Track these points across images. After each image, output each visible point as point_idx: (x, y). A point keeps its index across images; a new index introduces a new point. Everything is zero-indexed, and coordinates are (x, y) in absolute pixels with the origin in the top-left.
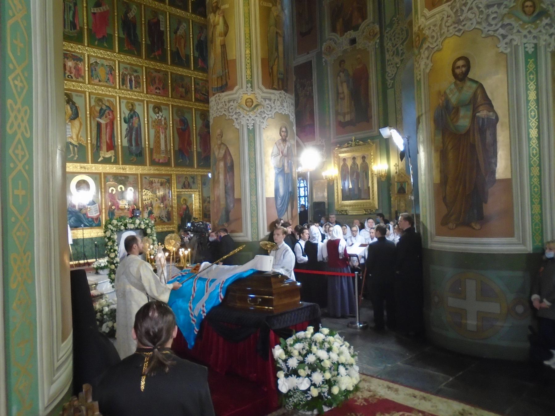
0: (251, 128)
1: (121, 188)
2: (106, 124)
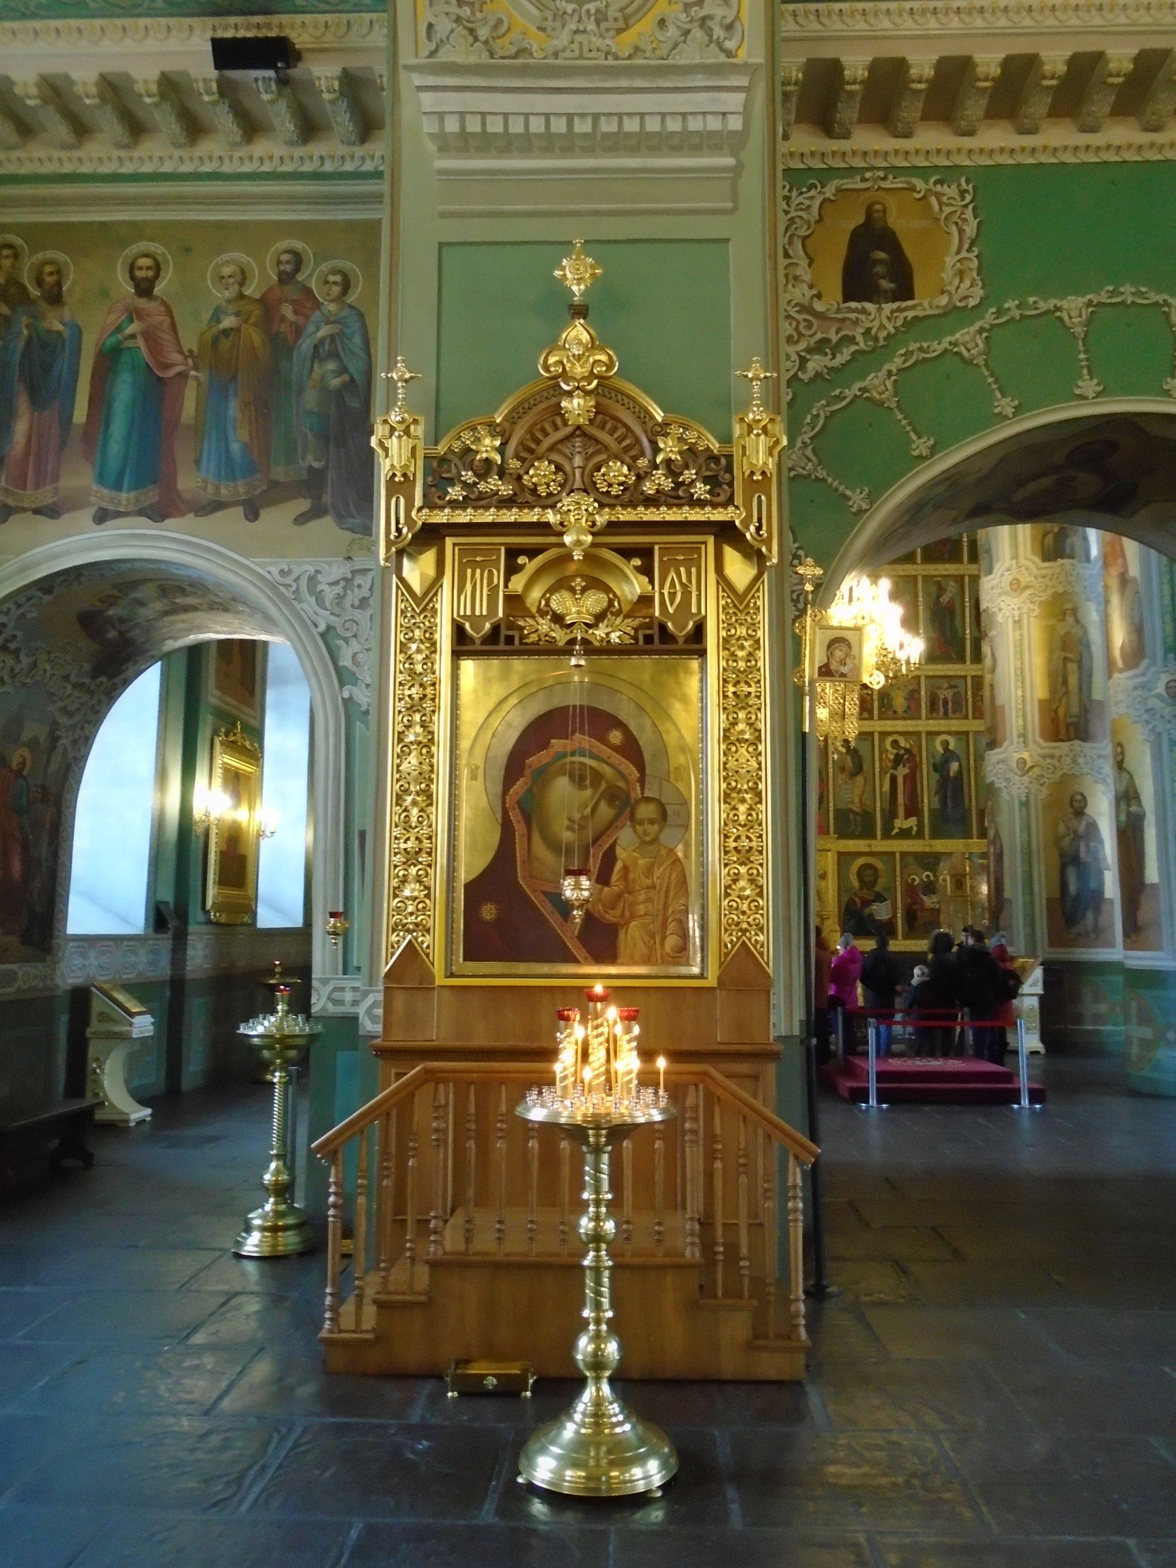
0: (1024, 799)
1: (928, 876)
2: (905, 777)
